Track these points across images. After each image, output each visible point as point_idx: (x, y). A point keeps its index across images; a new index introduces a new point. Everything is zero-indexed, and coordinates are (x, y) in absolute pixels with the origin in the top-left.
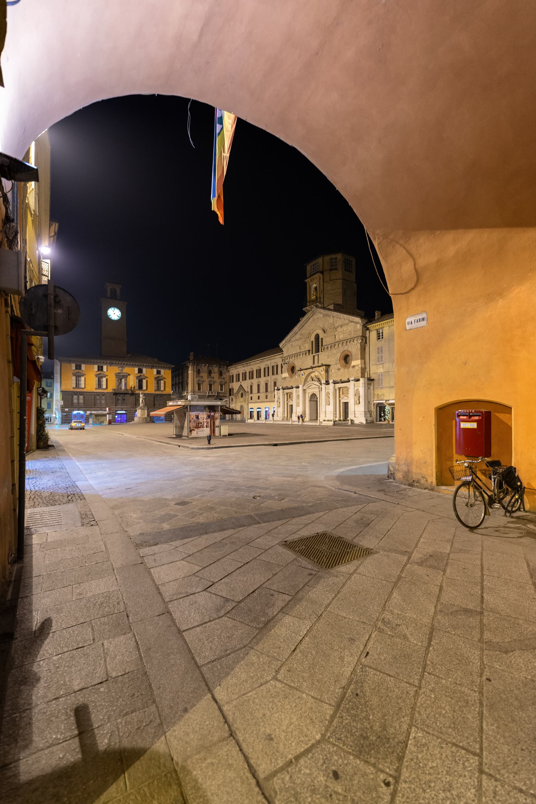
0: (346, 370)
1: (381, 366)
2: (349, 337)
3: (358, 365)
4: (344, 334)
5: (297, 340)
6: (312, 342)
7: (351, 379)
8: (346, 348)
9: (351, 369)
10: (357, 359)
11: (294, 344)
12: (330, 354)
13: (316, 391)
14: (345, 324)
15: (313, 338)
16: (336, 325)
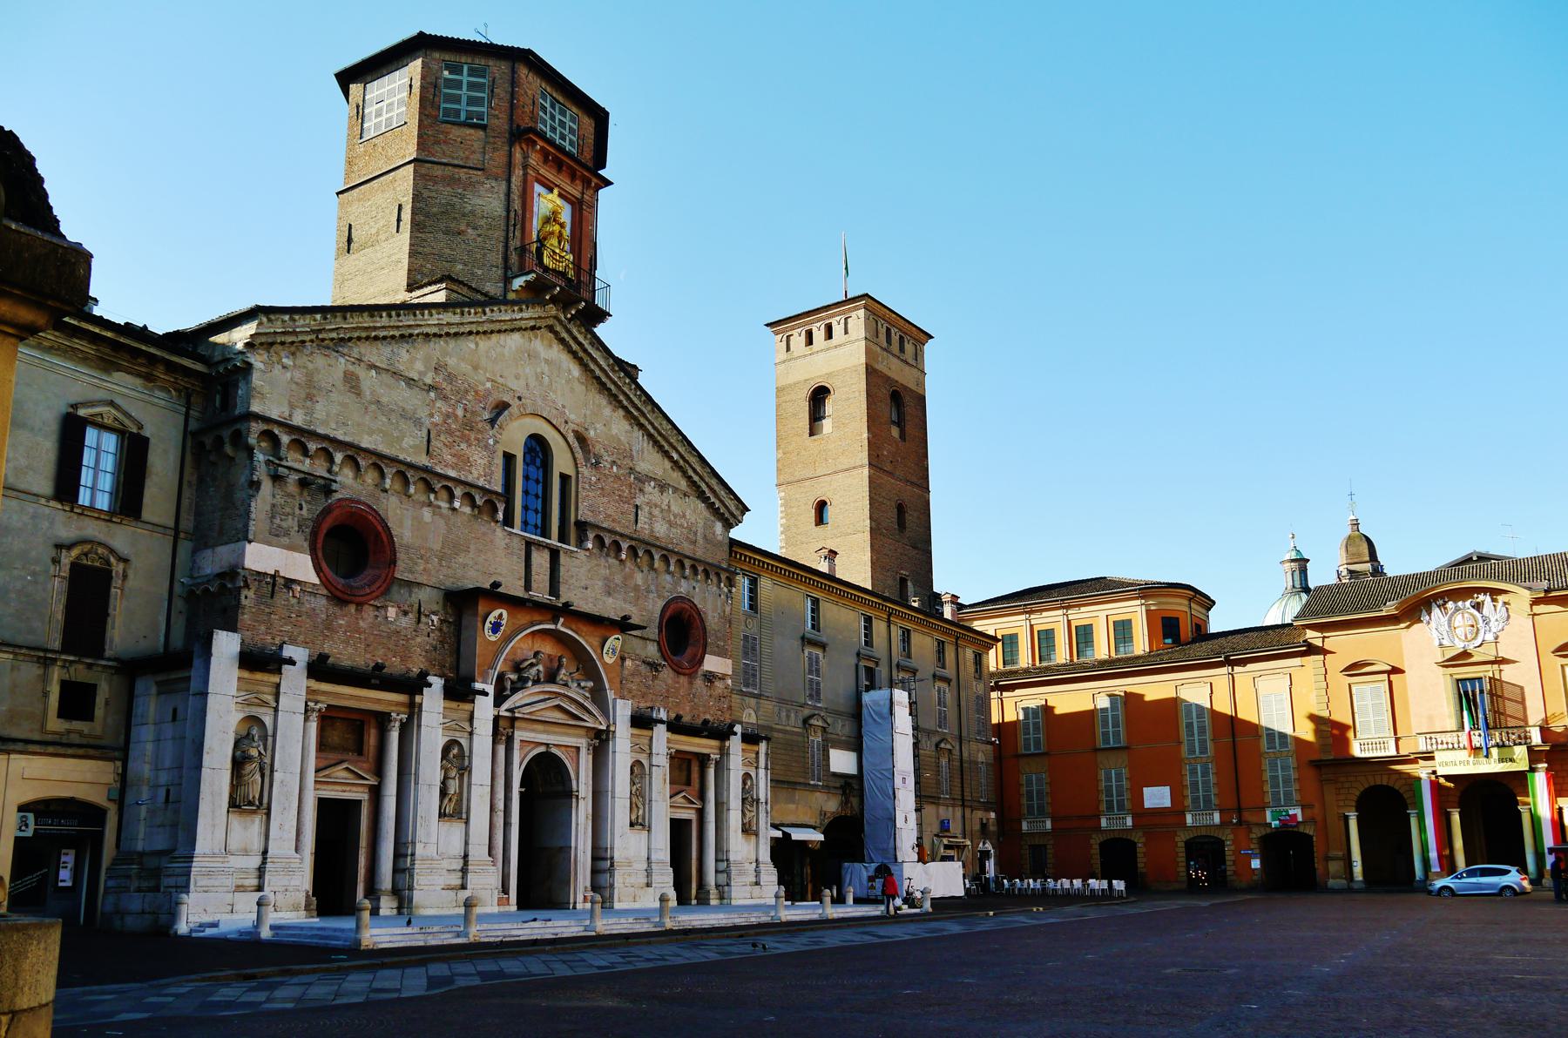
0: (683, 680)
1: (753, 701)
2: (686, 548)
3: (723, 678)
4: (671, 524)
5: (410, 382)
6: (509, 458)
7: (738, 728)
8: (684, 588)
9: (699, 682)
10: (722, 653)
11: (368, 379)
12: (618, 579)
13: (568, 743)
14: (676, 490)
15: (515, 434)
16: (643, 467)
